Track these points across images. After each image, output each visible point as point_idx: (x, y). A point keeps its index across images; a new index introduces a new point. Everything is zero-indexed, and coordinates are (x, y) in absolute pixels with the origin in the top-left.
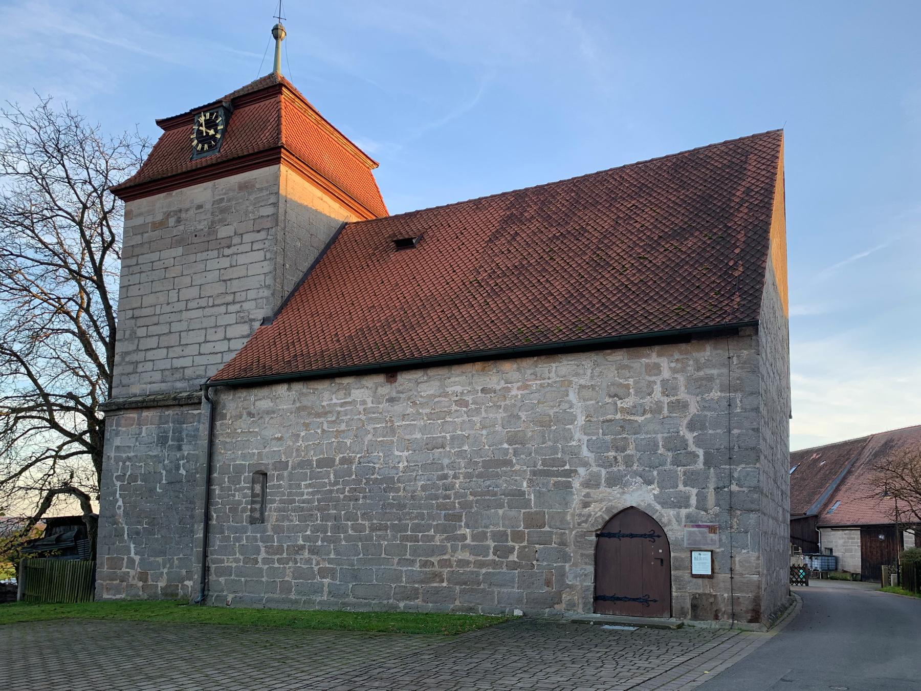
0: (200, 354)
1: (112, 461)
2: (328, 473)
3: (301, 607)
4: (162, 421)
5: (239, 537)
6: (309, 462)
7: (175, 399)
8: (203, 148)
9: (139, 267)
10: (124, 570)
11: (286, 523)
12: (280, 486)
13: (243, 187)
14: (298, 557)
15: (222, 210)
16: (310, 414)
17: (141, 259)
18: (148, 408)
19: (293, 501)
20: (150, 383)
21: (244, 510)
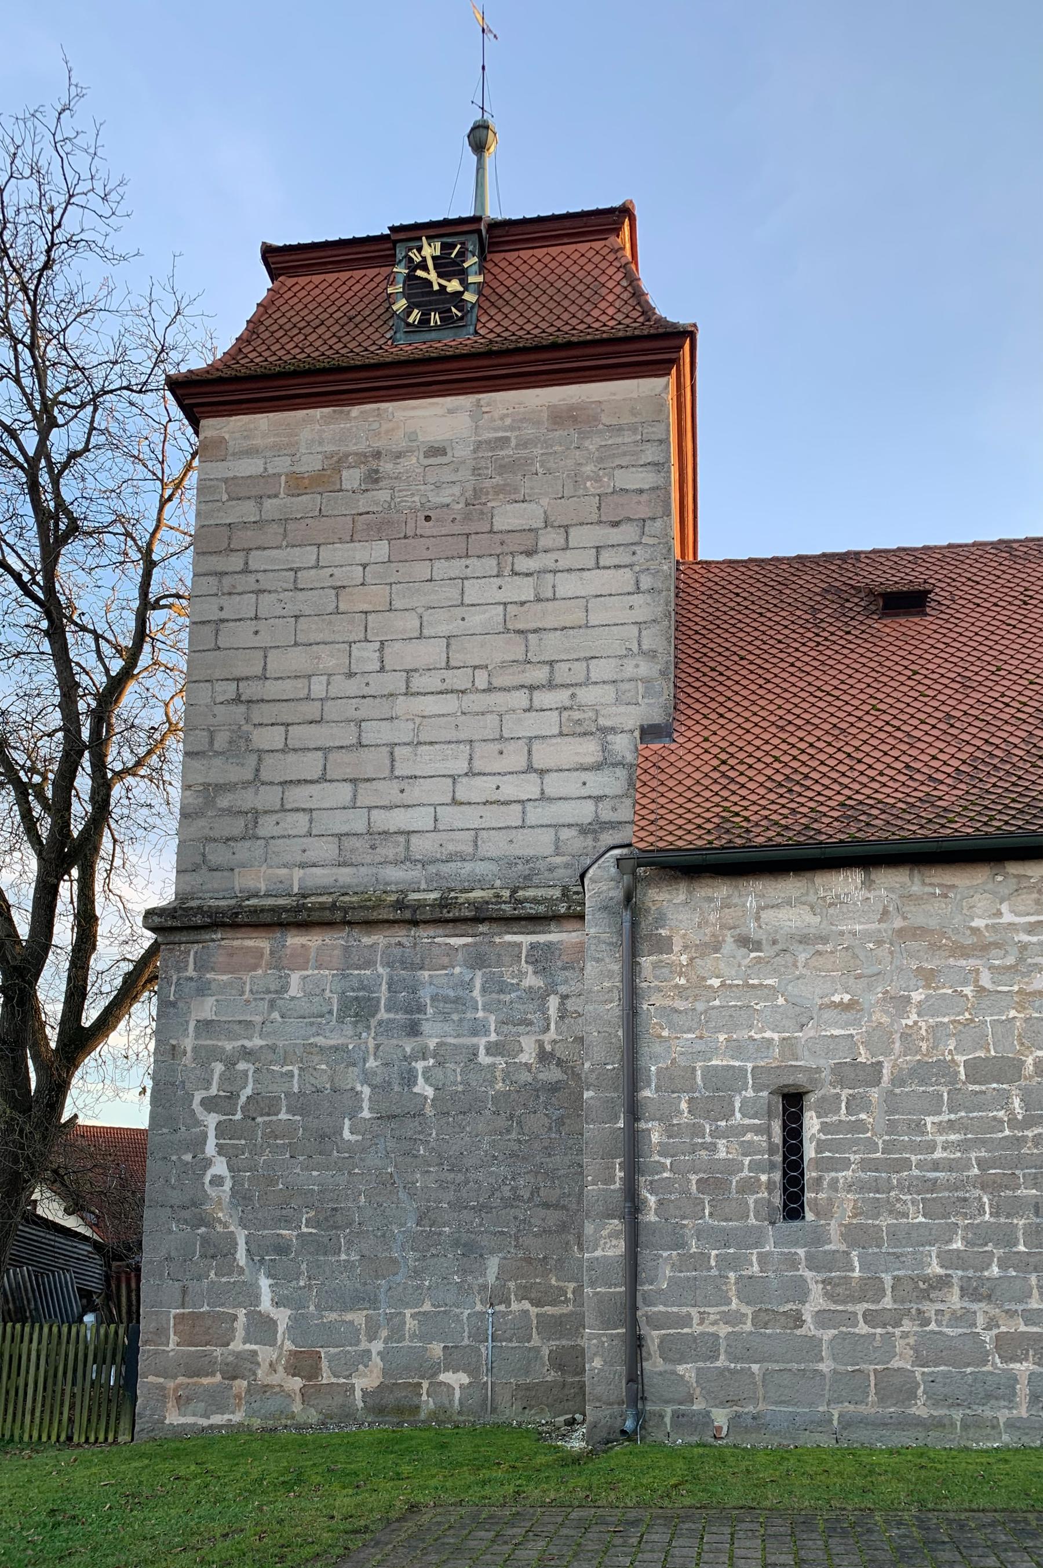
0: (455, 802)
1: (188, 1060)
2: (1007, 1096)
3: (955, 1439)
4: (349, 961)
5: (735, 1257)
6: (945, 1070)
7: (400, 905)
8: (424, 321)
9: (252, 578)
10: (237, 1345)
11: (885, 1221)
12: (859, 1127)
13: (560, 417)
14: (930, 1309)
15: (501, 466)
16: (934, 947)
17: (257, 560)
18: (305, 925)
19: (906, 1164)
20: (302, 866)
21: (749, 1186)
